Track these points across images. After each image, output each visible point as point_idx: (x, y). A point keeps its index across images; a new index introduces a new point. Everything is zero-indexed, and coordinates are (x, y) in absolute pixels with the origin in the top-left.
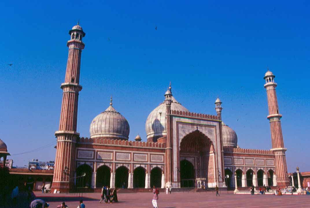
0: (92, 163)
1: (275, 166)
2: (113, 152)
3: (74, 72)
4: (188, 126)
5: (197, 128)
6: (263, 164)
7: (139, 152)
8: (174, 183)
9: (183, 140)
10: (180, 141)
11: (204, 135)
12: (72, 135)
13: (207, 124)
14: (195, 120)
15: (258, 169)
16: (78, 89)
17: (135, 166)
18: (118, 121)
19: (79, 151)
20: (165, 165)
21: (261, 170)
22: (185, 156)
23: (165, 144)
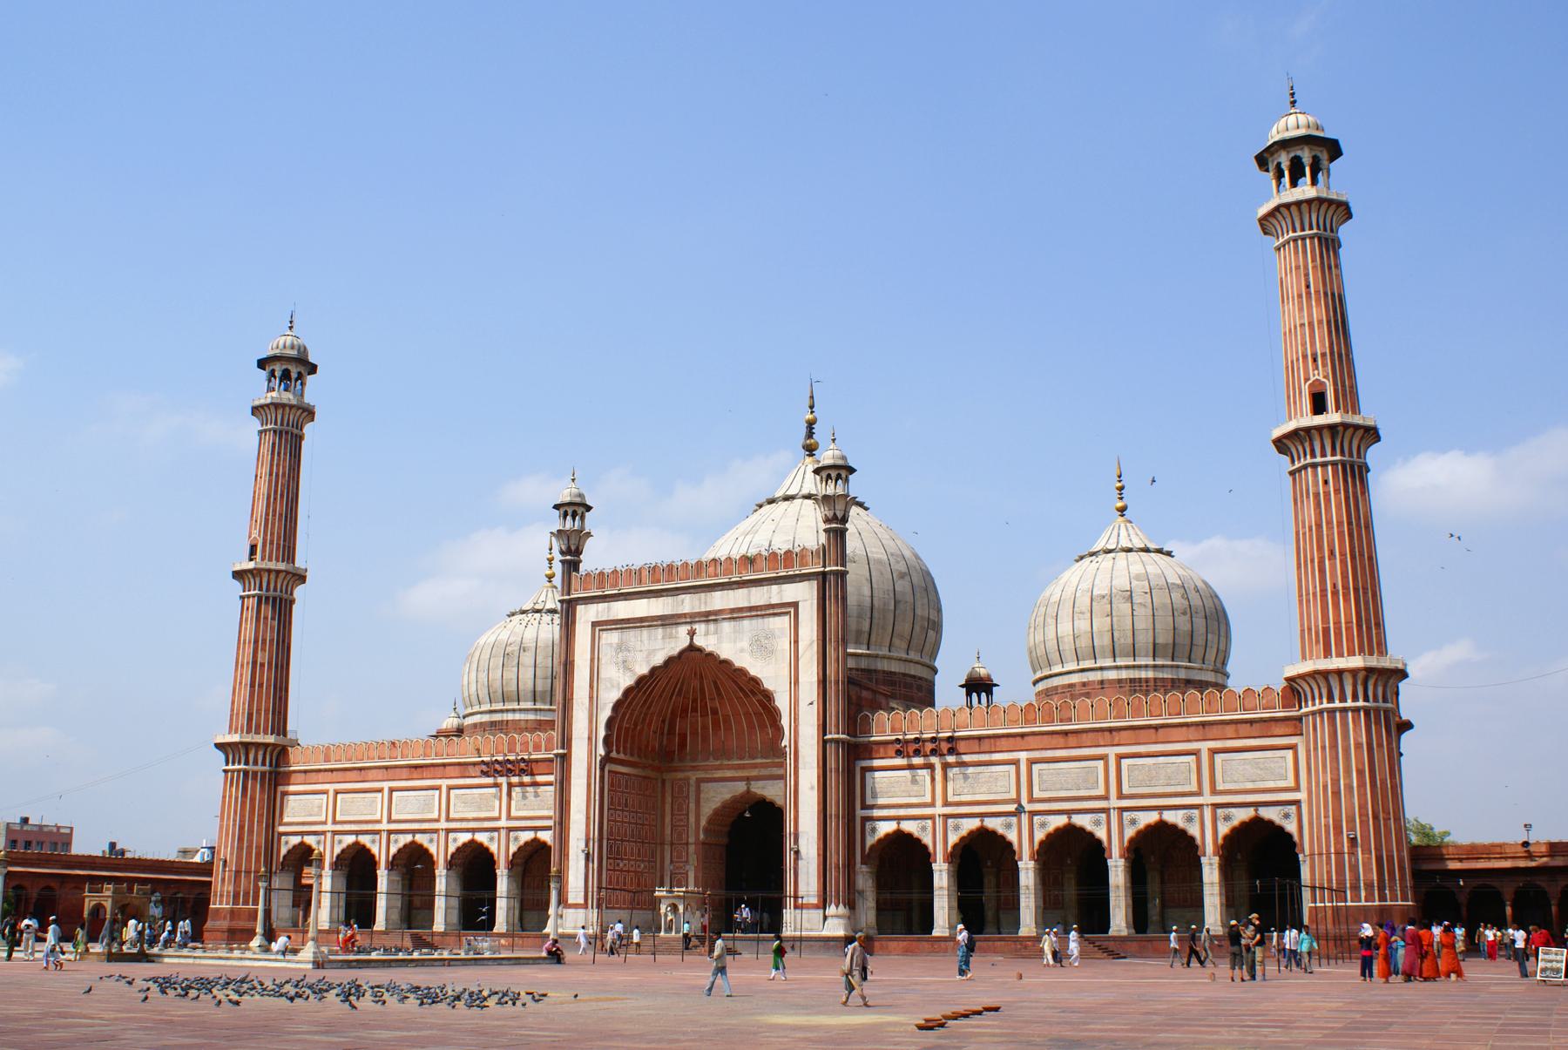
0: (323, 837)
1: (1301, 796)
2: (380, 790)
3: (256, 521)
4: (645, 632)
5: (692, 633)
6: (1187, 789)
8: (571, 911)
9: (617, 706)
10: (605, 714)
11: (727, 663)
12: (240, 746)
15: (1133, 822)
16: (273, 576)
17: (455, 840)
18: (509, 649)
21: (1161, 825)
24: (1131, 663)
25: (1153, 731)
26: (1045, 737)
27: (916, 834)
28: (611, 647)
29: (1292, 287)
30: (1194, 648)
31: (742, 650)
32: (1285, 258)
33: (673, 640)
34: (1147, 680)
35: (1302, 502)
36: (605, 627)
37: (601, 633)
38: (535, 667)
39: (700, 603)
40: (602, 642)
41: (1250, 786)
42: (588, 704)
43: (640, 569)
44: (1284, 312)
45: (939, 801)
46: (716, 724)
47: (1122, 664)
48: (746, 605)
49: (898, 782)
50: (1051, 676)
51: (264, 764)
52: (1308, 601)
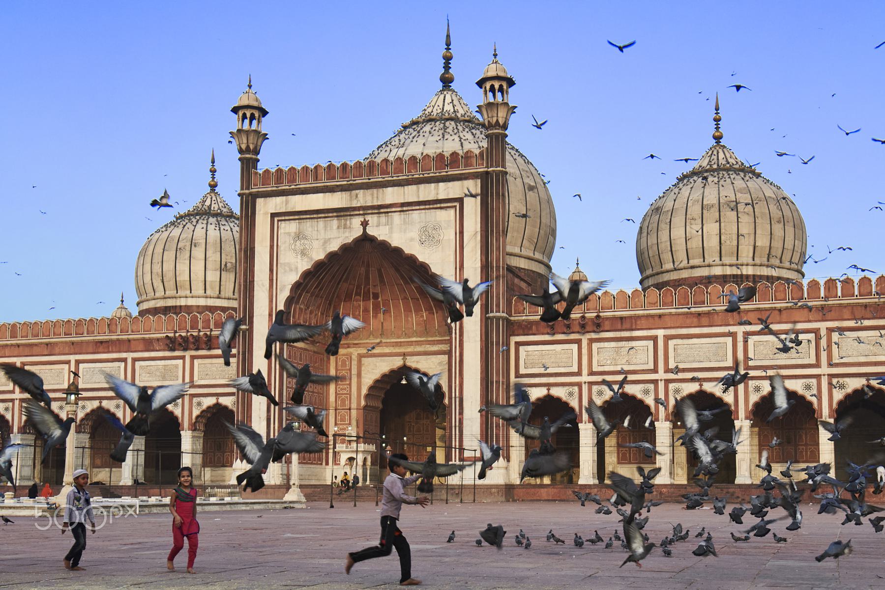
4: (321, 223)
5: (365, 224)
14: (354, 192)
22: (402, 350)
24: (734, 261)
25: (777, 312)
26: (680, 316)
27: (564, 399)
28: (290, 235)
30: (785, 251)
33: (348, 230)
34: (750, 275)
36: (283, 218)
38: (205, 260)
39: (373, 198)
41: (863, 359)
42: (268, 285)
43: (316, 167)
45: (585, 371)
46: (376, 308)
47: (728, 262)
48: (416, 200)
49: (548, 355)
50: (662, 273)
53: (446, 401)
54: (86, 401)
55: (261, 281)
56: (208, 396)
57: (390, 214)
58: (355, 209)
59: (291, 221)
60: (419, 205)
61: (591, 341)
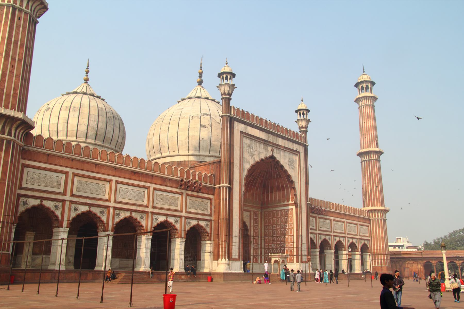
0: (61, 204)
1: (370, 238)
2: (110, 181)
4: (258, 144)
5: (273, 151)
7: (166, 188)
10: (245, 173)
11: (282, 167)
12: (18, 122)
13: (287, 146)
14: (270, 135)
19: (26, 170)
20: (213, 222)
23: (214, 176)
25: (351, 216)
28: (247, 145)
29: (372, 116)
31: (286, 163)
32: (369, 108)
35: (374, 168)
37: (243, 137)
38: (120, 129)
40: (244, 141)
41: (364, 235)
42: (239, 167)
44: (368, 121)
51: (21, 141)
52: (376, 192)
53: (249, 233)
54: (121, 211)
55: (236, 163)
56: (194, 219)
57: (280, 150)
58: (270, 142)
59: (247, 138)
60: (289, 150)
61: (319, 218)
